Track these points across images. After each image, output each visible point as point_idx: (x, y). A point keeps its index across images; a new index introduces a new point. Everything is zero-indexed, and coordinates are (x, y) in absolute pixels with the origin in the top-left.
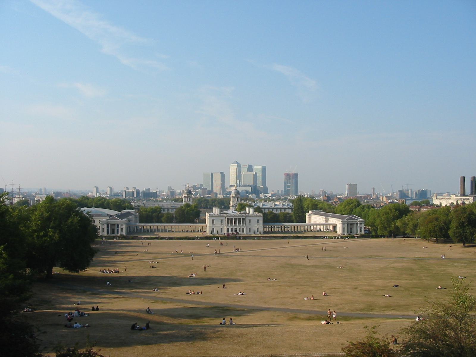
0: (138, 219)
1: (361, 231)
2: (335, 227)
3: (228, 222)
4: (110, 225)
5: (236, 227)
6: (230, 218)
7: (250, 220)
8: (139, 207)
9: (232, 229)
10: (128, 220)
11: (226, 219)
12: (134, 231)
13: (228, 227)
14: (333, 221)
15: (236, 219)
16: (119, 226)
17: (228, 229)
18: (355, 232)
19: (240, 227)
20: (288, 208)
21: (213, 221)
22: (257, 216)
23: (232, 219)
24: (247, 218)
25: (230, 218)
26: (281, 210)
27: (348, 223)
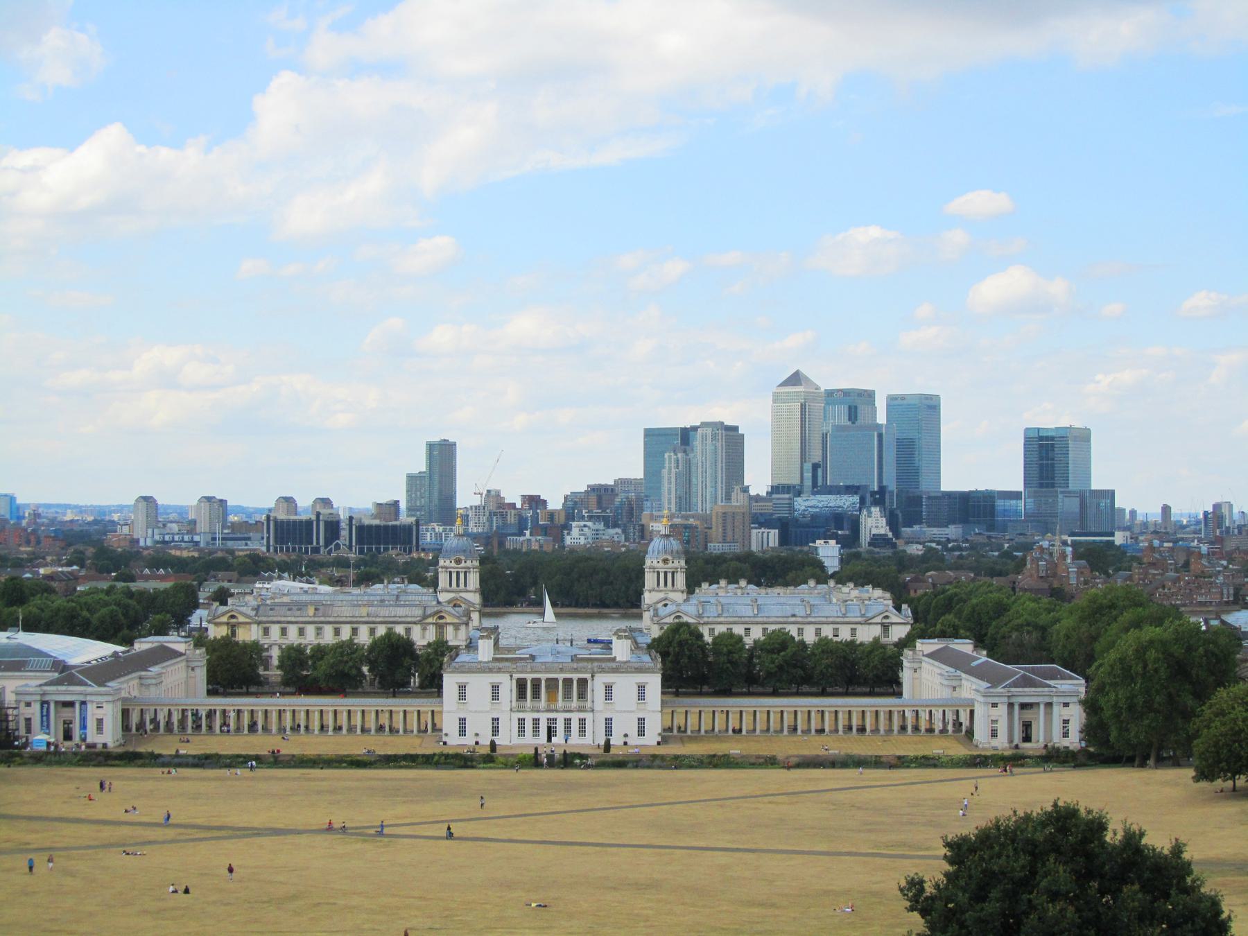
0: (201, 674)
1: (1066, 735)
2: (972, 712)
3: (521, 694)
4: (52, 706)
5: (552, 715)
6: (529, 677)
7: (609, 689)
8: (233, 617)
9: (536, 722)
10: (142, 684)
11: (514, 682)
12: (169, 724)
13: (521, 715)
14: (971, 688)
15: (552, 683)
16: (89, 706)
17: (521, 722)
18: (1041, 739)
19: (568, 715)
20: (867, 622)
21: (462, 688)
22: (640, 670)
23: (536, 684)
24: (597, 676)
25: (529, 677)
26: (818, 632)
27: (1013, 700)
